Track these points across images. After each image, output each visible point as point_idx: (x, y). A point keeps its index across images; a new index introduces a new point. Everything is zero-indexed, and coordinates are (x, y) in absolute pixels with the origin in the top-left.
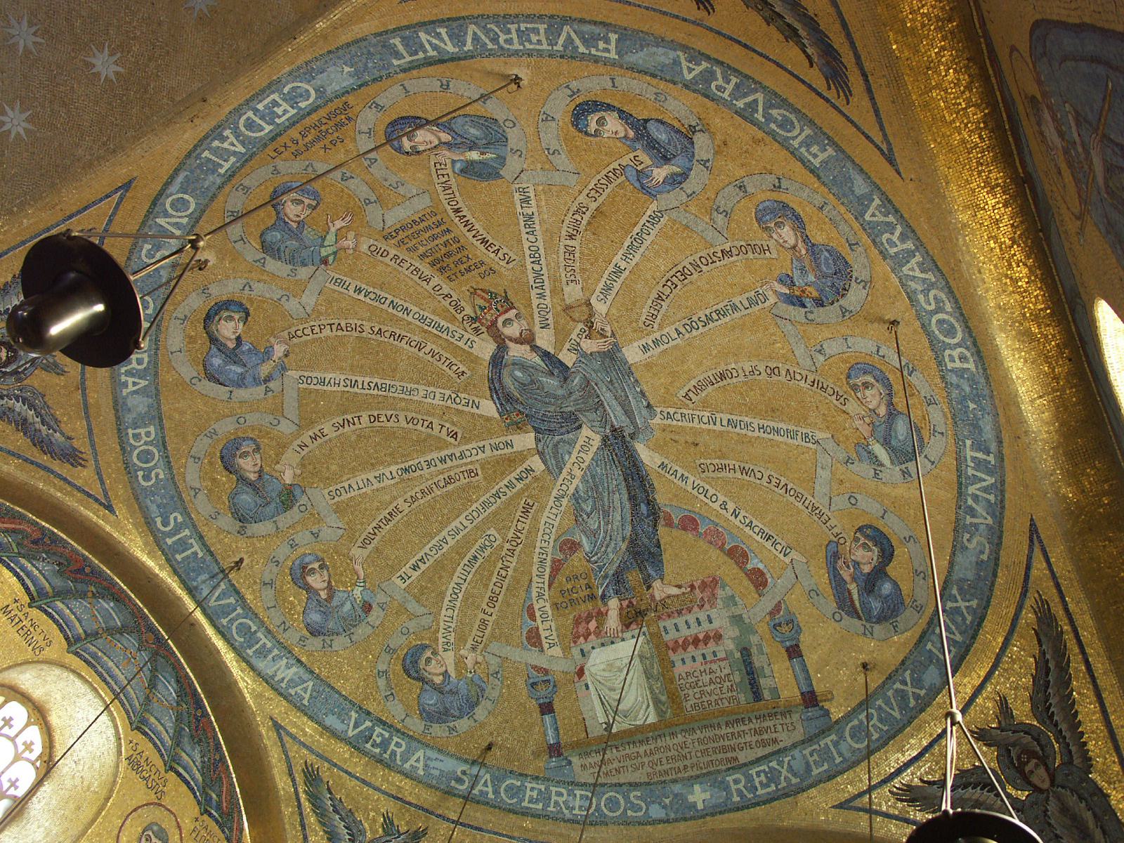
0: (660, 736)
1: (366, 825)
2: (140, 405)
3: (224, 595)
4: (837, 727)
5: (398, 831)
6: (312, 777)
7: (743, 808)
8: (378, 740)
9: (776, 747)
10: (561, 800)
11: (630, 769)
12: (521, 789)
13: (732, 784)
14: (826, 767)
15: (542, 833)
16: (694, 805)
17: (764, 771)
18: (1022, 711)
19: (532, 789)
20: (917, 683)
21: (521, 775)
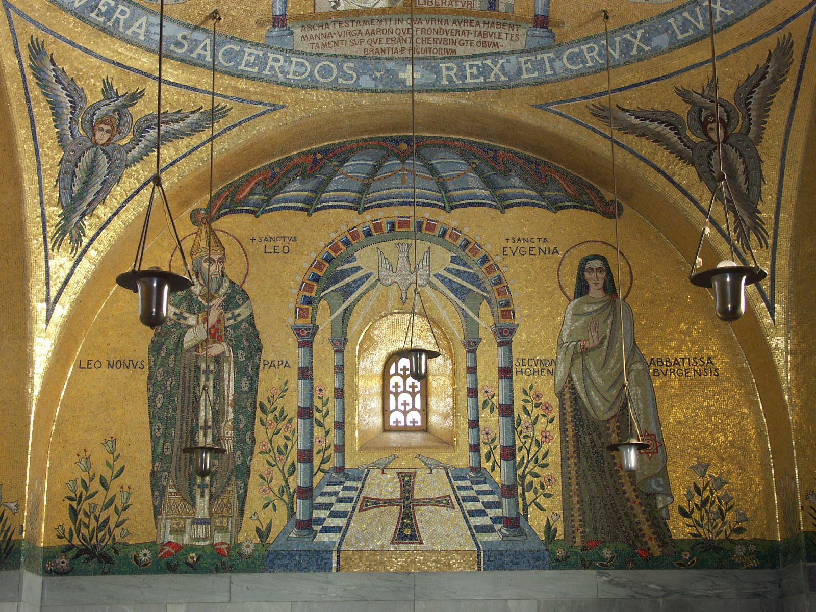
0: (386, 20)
1: (86, 92)
4: (558, 48)
5: (117, 94)
6: (36, 50)
7: (449, 91)
8: (104, 9)
9: (496, 50)
10: (277, 65)
11: (348, 43)
12: (240, 54)
13: (444, 70)
14: (536, 74)
15: (255, 93)
16: (404, 82)
17: (477, 66)
18: (726, 91)
19: (250, 54)
20: (646, 40)
21: (241, 41)
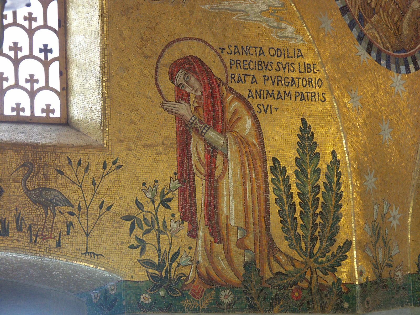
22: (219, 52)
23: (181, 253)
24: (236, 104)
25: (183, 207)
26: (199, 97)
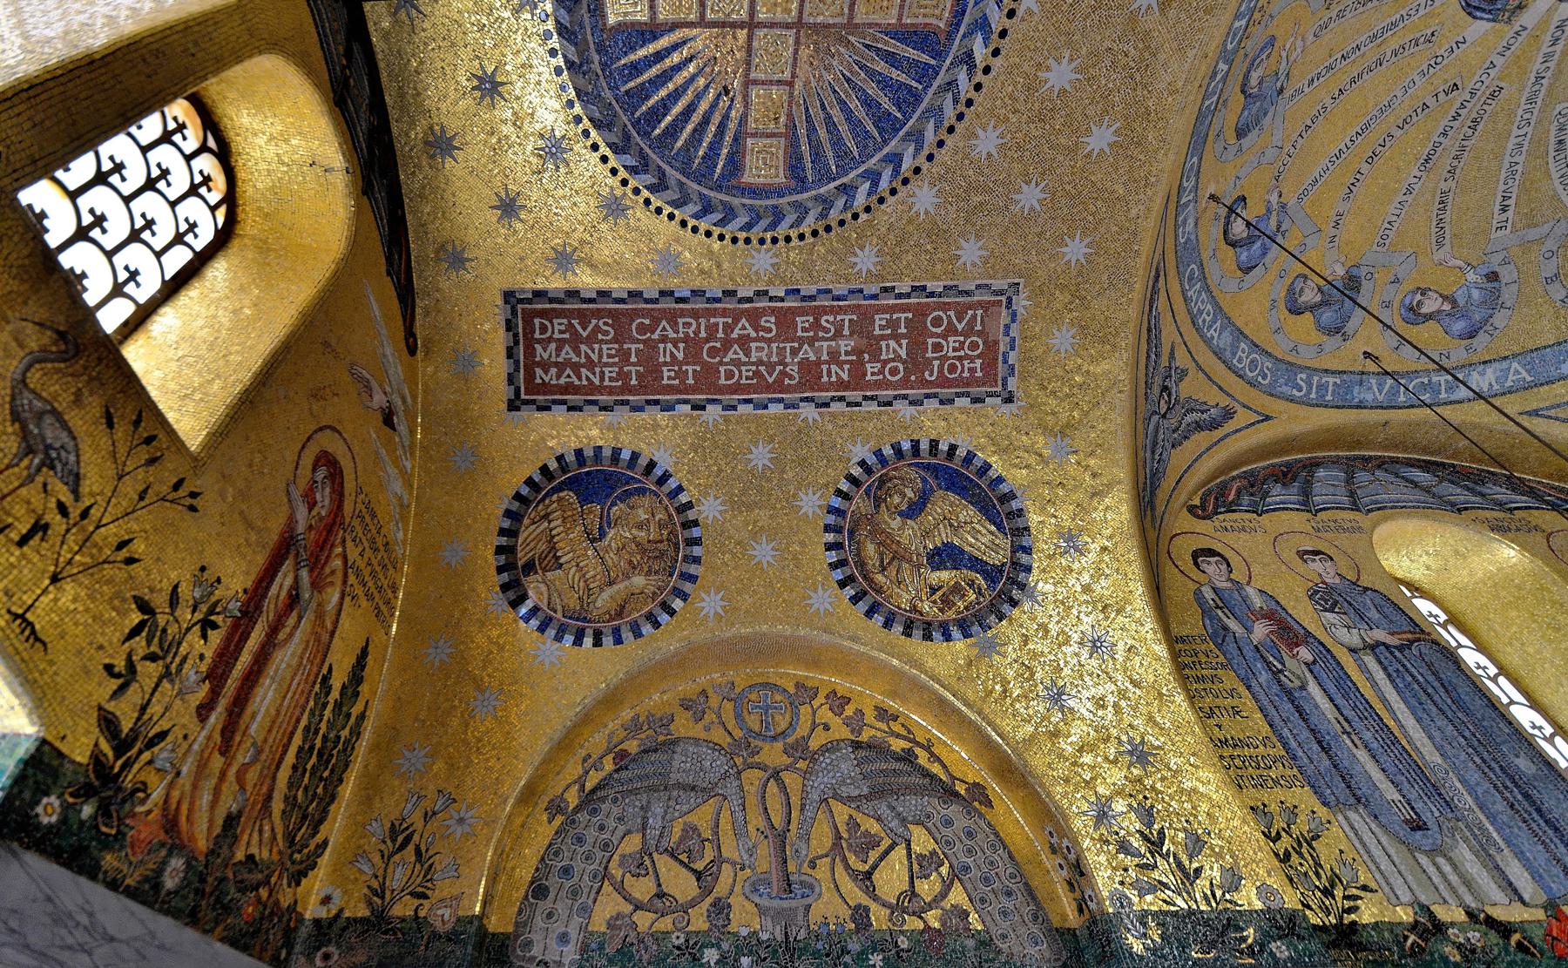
2: (1225, 340)
3: (1380, 385)
22: (359, 491)
23: (169, 738)
24: (338, 563)
25: (226, 656)
26: (321, 518)
